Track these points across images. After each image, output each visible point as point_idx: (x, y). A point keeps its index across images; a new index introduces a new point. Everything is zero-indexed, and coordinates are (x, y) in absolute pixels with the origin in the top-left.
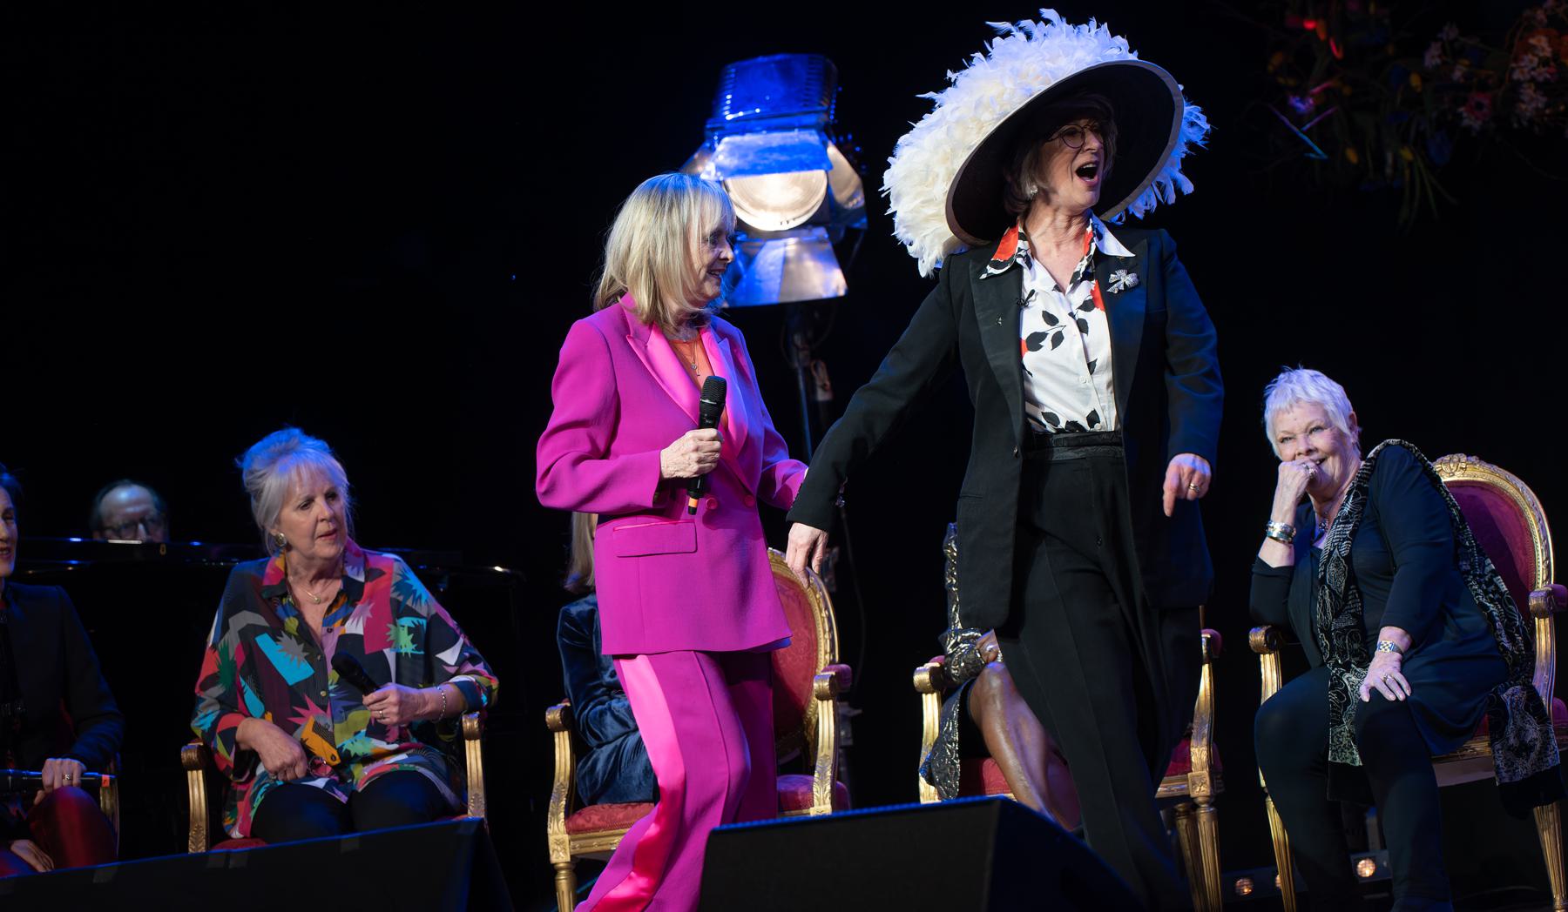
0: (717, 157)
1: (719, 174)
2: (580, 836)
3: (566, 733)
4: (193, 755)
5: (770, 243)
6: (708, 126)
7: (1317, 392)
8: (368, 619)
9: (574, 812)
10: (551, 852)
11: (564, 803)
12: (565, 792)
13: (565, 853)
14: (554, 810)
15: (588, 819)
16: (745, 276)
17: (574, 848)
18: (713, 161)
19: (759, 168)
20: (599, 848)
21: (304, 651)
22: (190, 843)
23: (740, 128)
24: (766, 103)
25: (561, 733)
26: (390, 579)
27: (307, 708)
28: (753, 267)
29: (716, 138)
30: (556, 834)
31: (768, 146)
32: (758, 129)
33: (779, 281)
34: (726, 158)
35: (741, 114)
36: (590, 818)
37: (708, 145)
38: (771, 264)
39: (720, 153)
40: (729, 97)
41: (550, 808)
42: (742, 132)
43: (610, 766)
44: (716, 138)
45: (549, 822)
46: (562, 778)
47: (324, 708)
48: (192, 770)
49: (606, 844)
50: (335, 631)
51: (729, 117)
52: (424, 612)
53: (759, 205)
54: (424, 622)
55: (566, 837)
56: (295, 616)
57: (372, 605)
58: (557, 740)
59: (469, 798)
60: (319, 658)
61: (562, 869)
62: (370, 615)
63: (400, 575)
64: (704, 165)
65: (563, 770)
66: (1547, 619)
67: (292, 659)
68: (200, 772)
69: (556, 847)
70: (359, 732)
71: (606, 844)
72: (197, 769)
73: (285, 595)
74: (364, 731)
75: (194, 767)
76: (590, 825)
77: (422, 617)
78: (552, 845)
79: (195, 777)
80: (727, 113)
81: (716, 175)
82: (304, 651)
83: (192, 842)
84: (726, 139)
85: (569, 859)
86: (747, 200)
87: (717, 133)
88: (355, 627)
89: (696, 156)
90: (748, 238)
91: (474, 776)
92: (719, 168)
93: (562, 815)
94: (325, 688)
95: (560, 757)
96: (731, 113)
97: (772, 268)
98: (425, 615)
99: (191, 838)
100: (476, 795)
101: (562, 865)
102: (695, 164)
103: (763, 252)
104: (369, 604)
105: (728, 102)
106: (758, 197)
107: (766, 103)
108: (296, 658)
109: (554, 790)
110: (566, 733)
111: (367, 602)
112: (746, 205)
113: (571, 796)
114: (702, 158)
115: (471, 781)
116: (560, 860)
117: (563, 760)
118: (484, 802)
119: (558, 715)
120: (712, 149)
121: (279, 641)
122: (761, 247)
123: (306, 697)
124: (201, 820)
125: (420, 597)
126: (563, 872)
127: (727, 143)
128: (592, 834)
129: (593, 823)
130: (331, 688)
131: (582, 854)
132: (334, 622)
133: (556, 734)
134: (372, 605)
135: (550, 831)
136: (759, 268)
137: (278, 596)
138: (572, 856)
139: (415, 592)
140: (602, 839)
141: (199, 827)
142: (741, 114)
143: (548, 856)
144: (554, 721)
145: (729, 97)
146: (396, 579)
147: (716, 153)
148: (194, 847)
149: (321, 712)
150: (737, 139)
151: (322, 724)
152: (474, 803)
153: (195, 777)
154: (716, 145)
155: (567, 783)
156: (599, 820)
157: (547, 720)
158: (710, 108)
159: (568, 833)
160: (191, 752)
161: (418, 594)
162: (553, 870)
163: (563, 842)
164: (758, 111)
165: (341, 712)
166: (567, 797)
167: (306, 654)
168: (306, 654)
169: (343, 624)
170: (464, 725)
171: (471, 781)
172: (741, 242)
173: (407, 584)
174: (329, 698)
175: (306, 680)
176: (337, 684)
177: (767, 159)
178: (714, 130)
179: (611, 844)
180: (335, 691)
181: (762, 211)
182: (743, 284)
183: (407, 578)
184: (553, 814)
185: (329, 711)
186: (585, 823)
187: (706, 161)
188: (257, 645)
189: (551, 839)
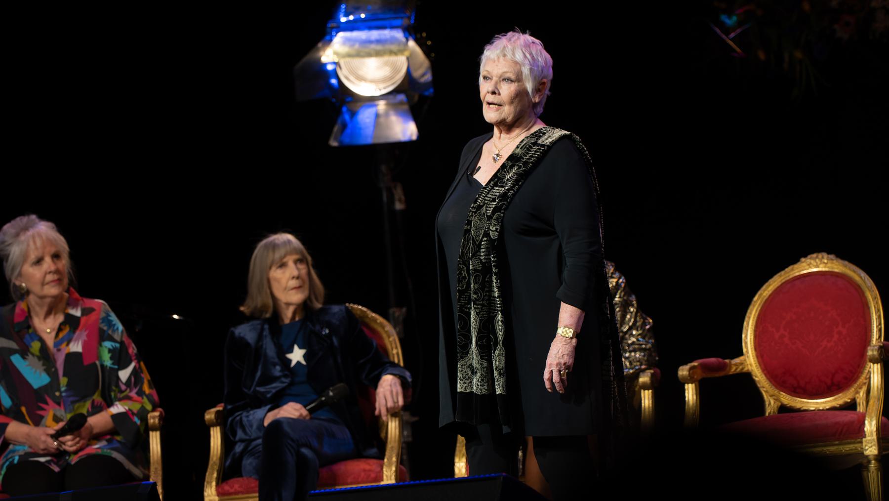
3: (218, 428)
9: (223, 481)
11: (215, 475)
12: (216, 467)
16: (350, 126)
23: (350, 27)
25: (215, 428)
27: (47, 403)
33: (372, 128)
35: (351, 18)
41: (206, 479)
46: (215, 459)
47: (59, 404)
51: (343, 20)
53: (361, 78)
58: (212, 433)
60: (53, 370)
62: (86, 339)
64: (324, 51)
76: (232, 491)
89: (320, 45)
92: (336, 53)
93: (214, 484)
94: (59, 390)
102: (318, 50)
106: (361, 73)
109: (210, 466)
110: (218, 428)
112: (352, 78)
120: (331, 40)
127: (342, 37)
130: (63, 389)
133: (212, 429)
135: (206, 494)
142: (351, 18)
144: (210, 420)
150: (348, 34)
155: (218, 462)
156: (239, 487)
158: (332, 14)
164: (363, 16)
166: (218, 471)
178: (333, 28)
180: (65, 391)
182: (348, 131)
183: (110, 316)
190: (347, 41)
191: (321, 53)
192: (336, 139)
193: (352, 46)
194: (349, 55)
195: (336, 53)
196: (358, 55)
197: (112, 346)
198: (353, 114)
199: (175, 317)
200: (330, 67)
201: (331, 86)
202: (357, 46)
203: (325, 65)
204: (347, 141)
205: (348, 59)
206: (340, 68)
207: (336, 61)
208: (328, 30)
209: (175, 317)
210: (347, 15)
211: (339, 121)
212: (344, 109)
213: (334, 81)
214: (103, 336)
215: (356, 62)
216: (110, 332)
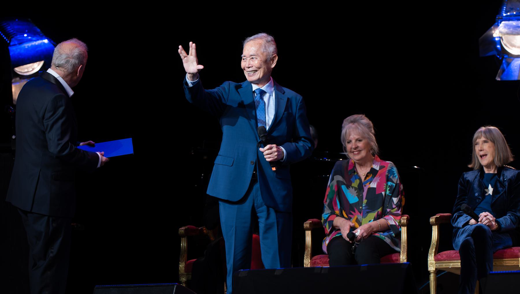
0: (500, 28)
1: (500, 34)
2: (439, 262)
3: (436, 226)
4: (308, 226)
5: (516, 59)
6: (497, 17)
7: (295, 145)
8: (378, 182)
9: (438, 253)
10: (428, 267)
11: (434, 250)
12: (435, 246)
13: (433, 267)
14: (431, 253)
15: (442, 256)
16: (506, 70)
17: (437, 266)
18: (498, 30)
19: (514, 33)
20: (445, 267)
21: (356, 193)
22: (305, 255)
23: (508, 19)
24: (518, 10)
25: (435, 226)
26: (386, 169)
27: (355, 212)
28: (509, 67)
29: (499, 22)
30: (430, 261)
31: (518, 25)
32: (514, 19)
33: (518, 72)
34: (503, 28)
35: (509, 14)
36: (443, 256)
37: (496, 24)
38: (516, 66)
39: (501, 27)
40: (505, 8)
41: (429, 252)
42: (509, 20)
43: (454, 239)
44: (499, 22)
45: (428, 257)
46: (434, 242)
47: (360, 213)
48: (307, 230)
49: (448, 266)
50: (367, 186)
51: (504, 15)
52: (395, 181)
53: (513, 46)
54: (394, 185)
55: (434, 262)
56: (358, 179)
57: (380, 178)
58: (433, 228)
59: (401, 246)
60: (361, 195)
61: (432, 273)
62: (379, 181)
63: (391, 167)
64: (495, 31)
65: (434, 239)
66: (185, 238)
67: (352, 195)
68: (310, 231)
69: (430, 265)
70: (371, 220)
71: (448, 266)
72: (309, 230)
73: (355, 172)
74: (372, 220)
75: (308, 229)
76: (442, 259)
77: (394, 183)
78: (429, 265)
79: (308, 233)
80: (504, 13)
81: (499, 35)
82: (356, 193)
83: (306, 255)
84: (503, 22)
85: (434, 270)
86: (509, 44)
87: (500, 20)
88: (374, 185)
89: (492, 27)
90: (508, 57)
91: (404, 239)
92: (500, 32)
93: (433, 254)
94: (362, 206)
95: (434, 234)
96: (505, 13)
97: (516, 68)
98: (395, 182)
99: (305, 254)
100: (404, 246)
101: (432, 272)
102: (492, 30)
103: (513, 61)
104: (379, 177)
105: (3, 36)
106: (513, 43)
107: (518, 10)
108: (353, 195)
109: (431, 246)
110: (436, 226)
111: (378, 177)
112: (508, 45)
113: (437, 248)
114: (494, 28)
115: (402, 241)
116: (432, 270)
117: (435, 236)
118: (406, 248)
119: (434, 220)
120: (498, 26)
121: (348, 189)
122: (513, 60)
123: (355, 208)
124: (309, 248)
125: (396, 176)
126: (432, 274)
127: (503, 24)
128: (443, 262)
129: (444, 258)
130: (364, 206)
131: (439, 268)
132: (367, 183)
133: (433, 226)
134: (380, 178)
135: (429, 259)
136: (511, 67)
137: (353, 173)
138: (436, 269)
139: (394, 174)
140: (455, 263)
141: (308, 250)
142: (509, 14)
143: (427, 268)
144: (433, 222)
145: (505, 8)
146: (388, 168)
147: (499, 27)
148: (306, 257)
149: (360, 214)
150: (507, 22)
151: (359, 219)
152: (403, 248)
153: (308, 233)
154: (499, 24)
155: (435, 244)
156: (446, 257)
157: (430, 221)
158: (498, 11)
159: (435, 261)
160: (307, 224)
161: (395, 175)
162: (429, 273)
163: (433, 264)
164: (515, 13)
165: (365, 214)
166: (435, 248)
167: (357, 194)
168: (357, 194)
169: (370, 184)
170: (401, 221)
171: (402, 241)
172: (506, 58)
173: (393, 171)
174: (363, 209)
175: (356, 203)
176: (366, 204)
177: (517, 30)
178: (499, 19)
179: (450, 266)
180: (365, 206)
181: (514, 48)
182: (505, 73)
183: (393, 169)
184: (430, 254)
185: (362, 214)
186: (441, 258)
187: (496, 29)
188: (341, 188)
189: (429, 262)
190: (506, 26)
191: (493, 32)
192: (499, 77)
193: (509, 29)
194: (507, 34)
195: (500, 32)
196: (512, 34)
197: (391, 184)
198: (509, 64)
199: (416, 167)
200: (497, 39)
201: (497, 49)
202: (511, 29)
203: (495, 38)
204: (505, 78)
205: (506, 36)
206: (502, 40)
207: (501, 36)
208: (497, 20)
209: (416, 167)
210: (506, 12)
211: (502, 67)
212: (504, 61)
213: (498, 46)
214: (388, 179)
215: (511, 37)
216: (391, 177)
